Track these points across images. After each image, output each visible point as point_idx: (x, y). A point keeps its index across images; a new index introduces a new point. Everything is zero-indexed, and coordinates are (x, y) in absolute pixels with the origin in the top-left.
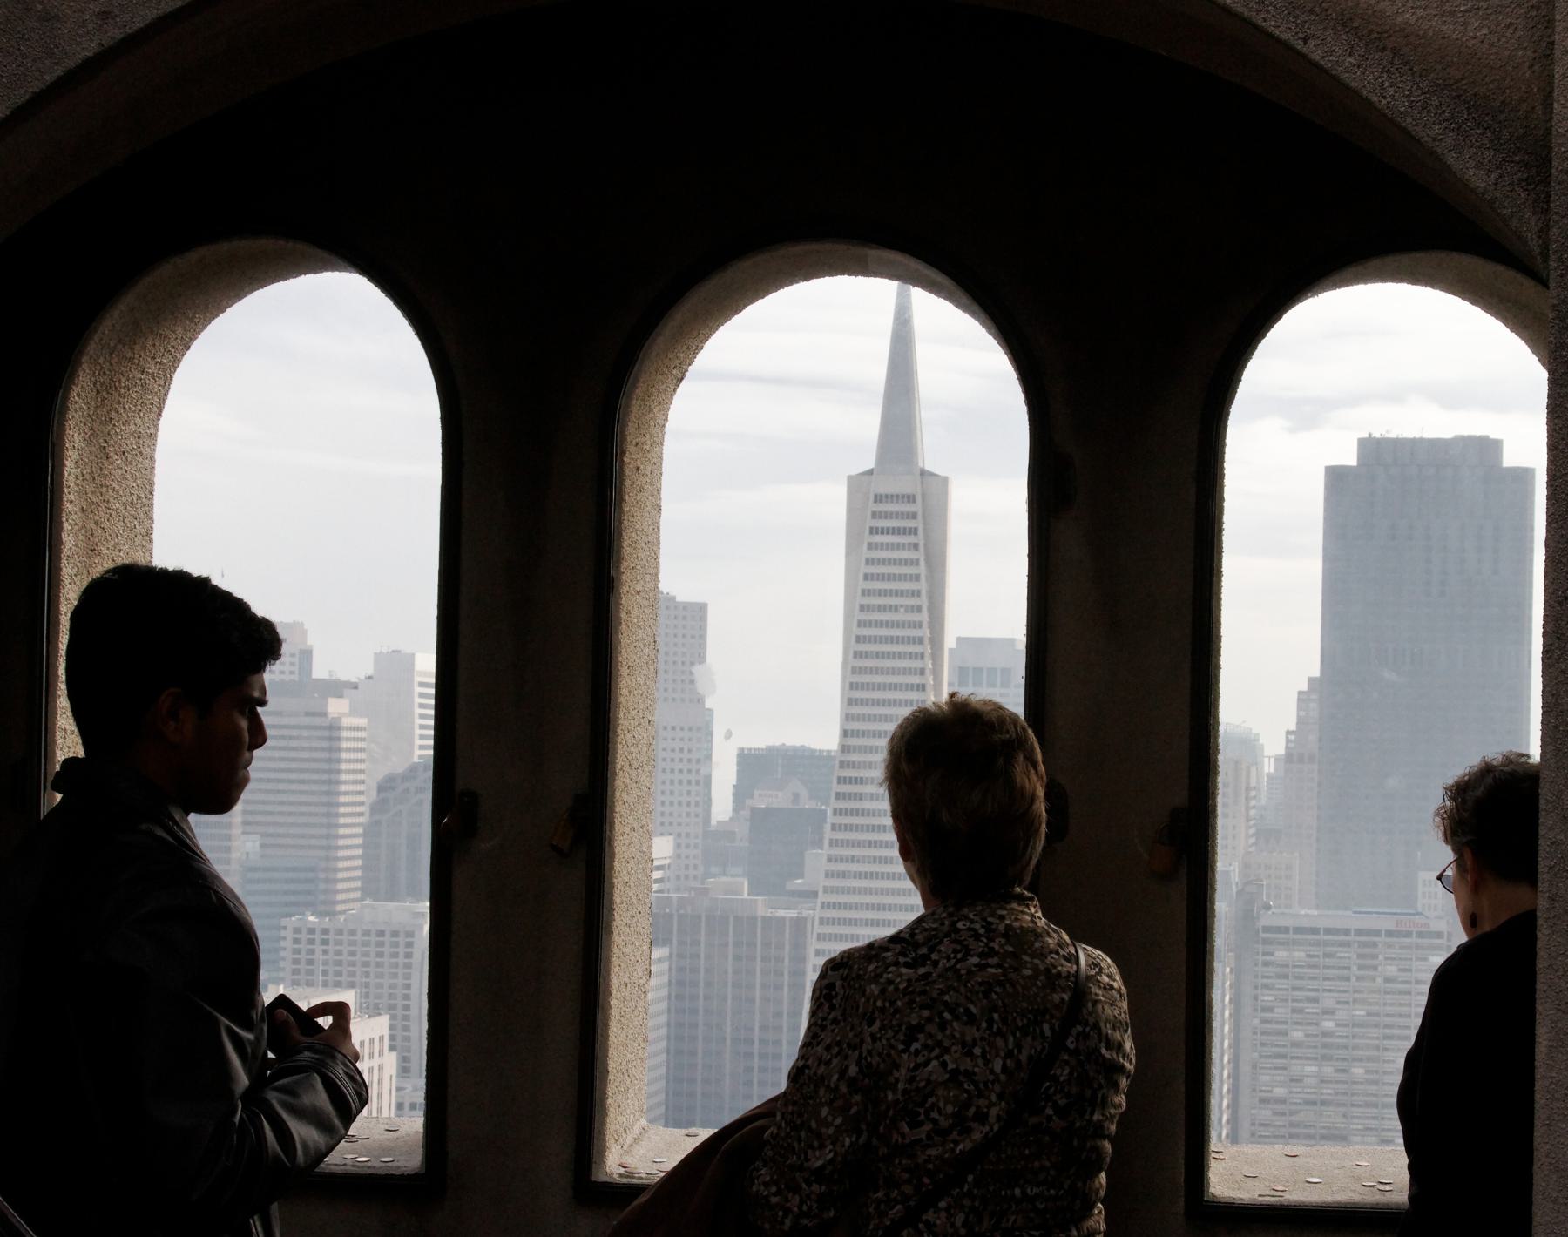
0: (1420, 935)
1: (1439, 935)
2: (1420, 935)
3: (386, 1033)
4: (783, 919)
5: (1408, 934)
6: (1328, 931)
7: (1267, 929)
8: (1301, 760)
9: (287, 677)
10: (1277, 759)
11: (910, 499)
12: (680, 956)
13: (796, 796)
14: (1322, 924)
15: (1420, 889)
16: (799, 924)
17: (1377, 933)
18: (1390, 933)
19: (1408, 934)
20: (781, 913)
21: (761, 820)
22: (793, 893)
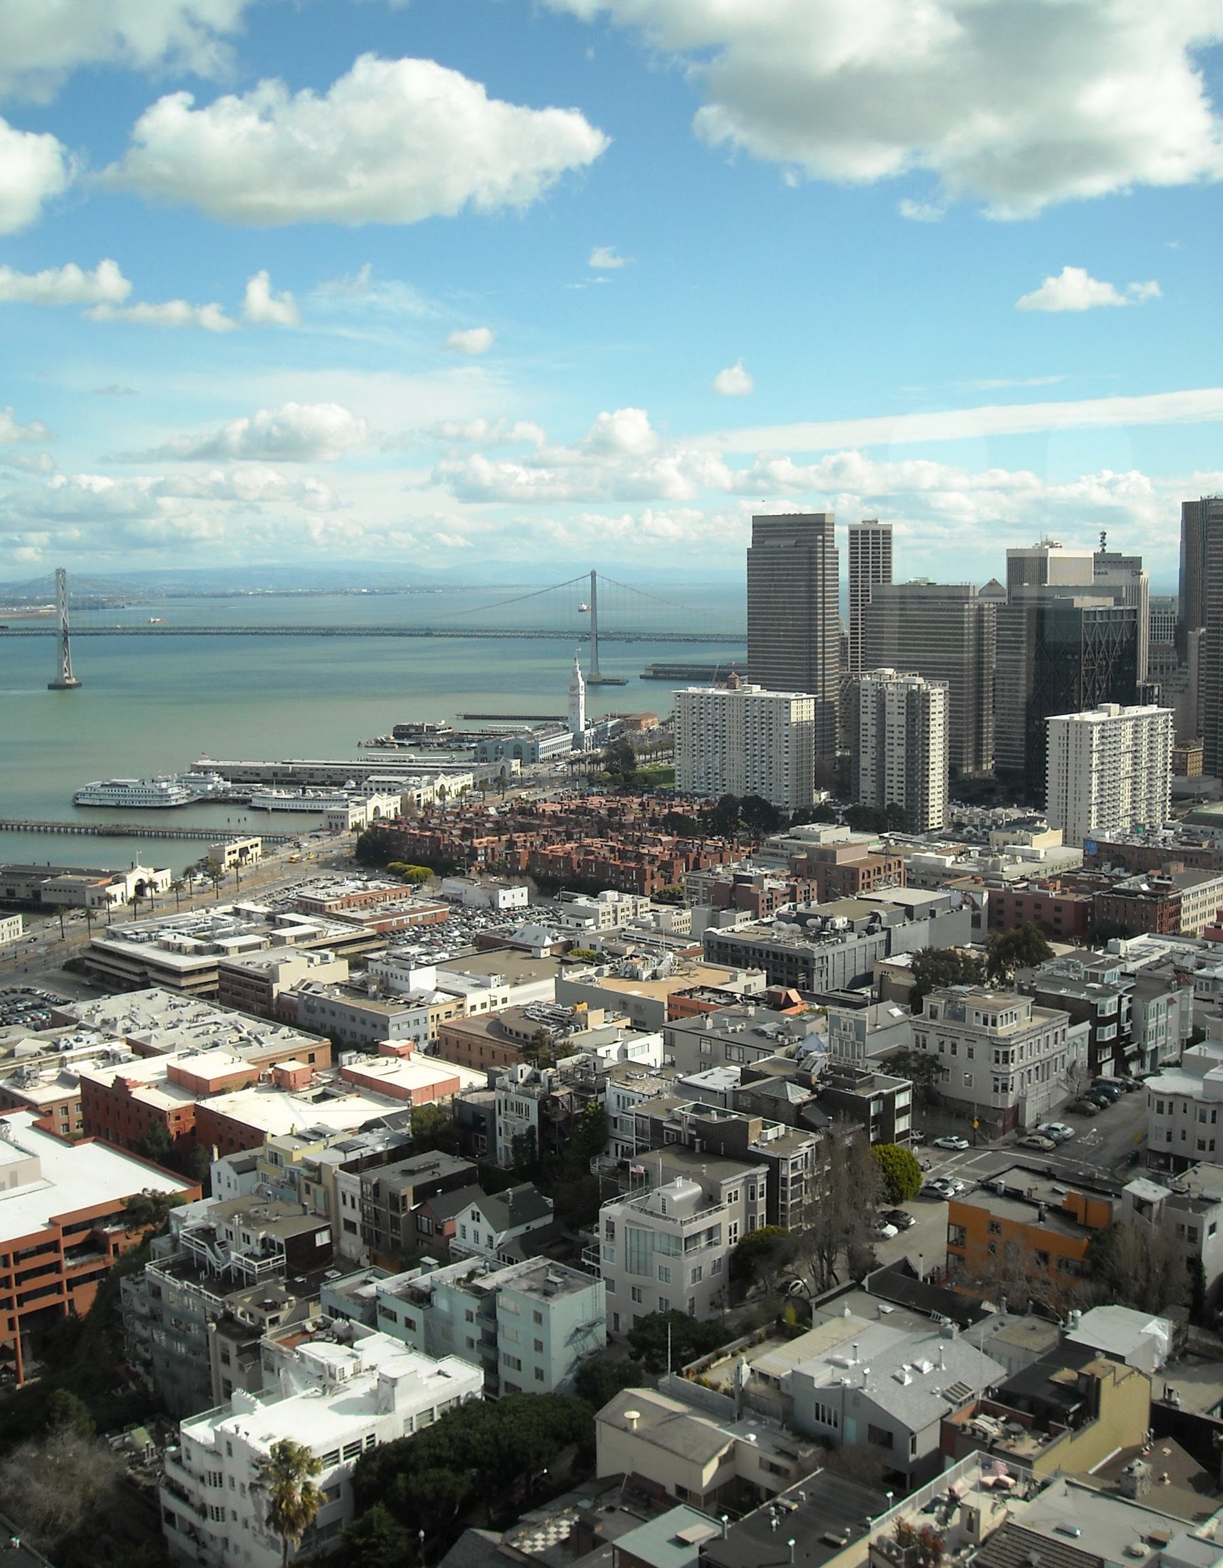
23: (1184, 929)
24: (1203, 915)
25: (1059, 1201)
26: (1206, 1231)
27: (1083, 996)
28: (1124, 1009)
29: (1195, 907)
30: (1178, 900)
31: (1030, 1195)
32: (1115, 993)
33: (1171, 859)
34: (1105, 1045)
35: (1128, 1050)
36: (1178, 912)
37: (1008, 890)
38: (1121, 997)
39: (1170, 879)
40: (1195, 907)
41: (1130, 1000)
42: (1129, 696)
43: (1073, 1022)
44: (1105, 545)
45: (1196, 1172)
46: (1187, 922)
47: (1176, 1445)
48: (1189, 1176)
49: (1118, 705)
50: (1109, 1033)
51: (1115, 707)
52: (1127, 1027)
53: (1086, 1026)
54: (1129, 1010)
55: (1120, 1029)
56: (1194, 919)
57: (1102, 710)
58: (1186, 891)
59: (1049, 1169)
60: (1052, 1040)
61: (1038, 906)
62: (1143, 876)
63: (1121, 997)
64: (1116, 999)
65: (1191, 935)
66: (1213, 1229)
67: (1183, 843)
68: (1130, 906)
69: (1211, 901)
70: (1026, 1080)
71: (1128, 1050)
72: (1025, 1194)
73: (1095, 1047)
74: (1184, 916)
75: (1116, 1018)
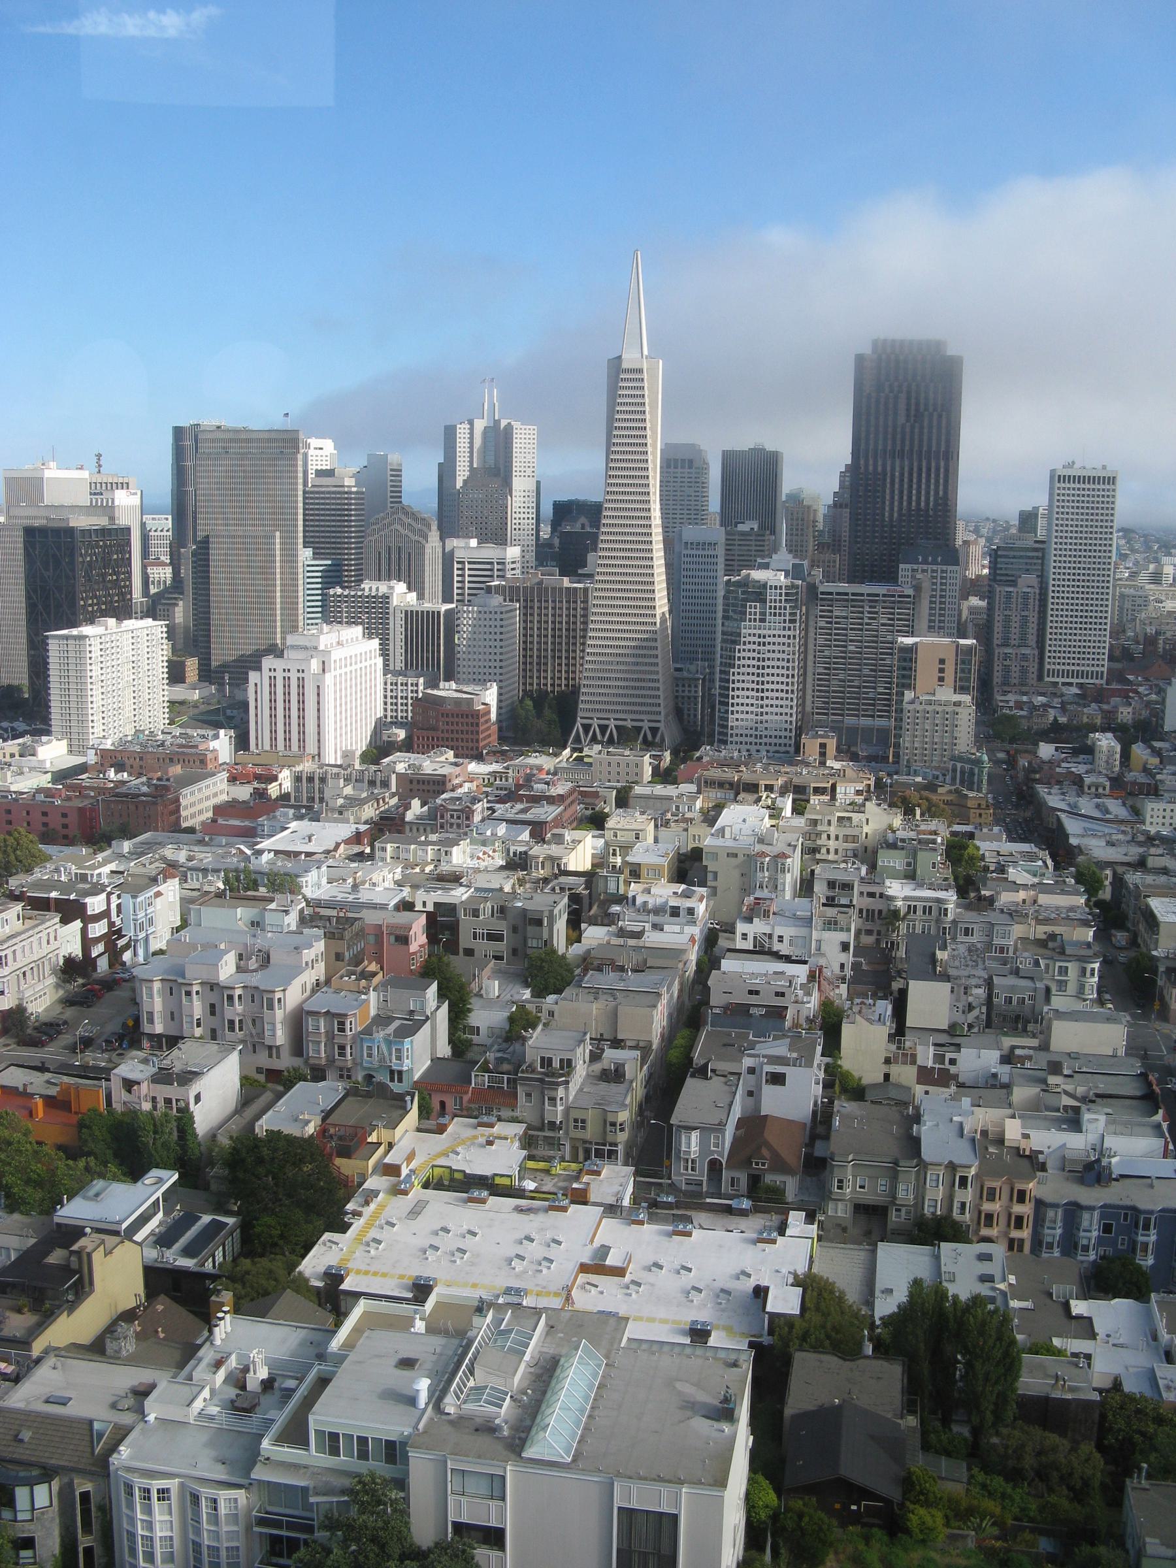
0: (900, 596)
1: (909, 596)
2: (900, 596)
3: (378, 647)
4: (575, 589)
5: (893, 596)
6: (853, 594)
7: (822, 593)
8: (841, 506)
9: (324, 468)
10: (829, 506)
11: (640, 371)
12: (525, 607)
13: (583, 527)
14: (850, 591)
15: (900, 573)
16: (586, 590)
17: (878, 595)
18: (884, 595)
19: (893, 596)
20: (575, 585)
21: (564, 537)
22: (581, 575)
23: (184, 825)
24: (201, 812)
25: (53, 1091)
26: (192, 1101)
27: (72, 897)
28: (113, 906)
29: (193, 805)
30: (177, 800)
31: (25, 1089)
32: (104, 891)
33: (171, 760)
34: (97, 940)
35: (121, 943)
36: (177, 810)
37: (16, 800)
38: (109, 894)
39: (168, 780)
40: (193, 805)
41: (119, 897)
42: (122, 611)
43: (65, 921)
44: (100, 466)
45: (180, 1049)
46: (186, 818)
47: (168, 1300)
48: (175, 1052)
49: (114, 620)
50: (98, 929)
51: (112, 621)
52: (118, 922)
53: (77, 924)
54: (119, 906)
55: (111, 924)
56: (193, 816)
57: (100, 624)
58: (185, 791)
59: (43, 1063)
60: (44, 941)
61: (45, 814)
62: (144, 779)
63: (109, 894)
64: (103, 896)
65: (191, 830)
66: (198, 1098)
67: (181, 746)
68: (132, 808)
69: (208, 798)
70: (22, 981)
71: (121, 943)
72: (21, 1089)
73: (87, 943)
74: (183, 813)
75: (106, 914)
